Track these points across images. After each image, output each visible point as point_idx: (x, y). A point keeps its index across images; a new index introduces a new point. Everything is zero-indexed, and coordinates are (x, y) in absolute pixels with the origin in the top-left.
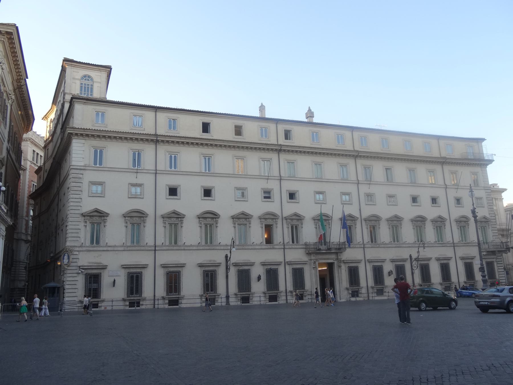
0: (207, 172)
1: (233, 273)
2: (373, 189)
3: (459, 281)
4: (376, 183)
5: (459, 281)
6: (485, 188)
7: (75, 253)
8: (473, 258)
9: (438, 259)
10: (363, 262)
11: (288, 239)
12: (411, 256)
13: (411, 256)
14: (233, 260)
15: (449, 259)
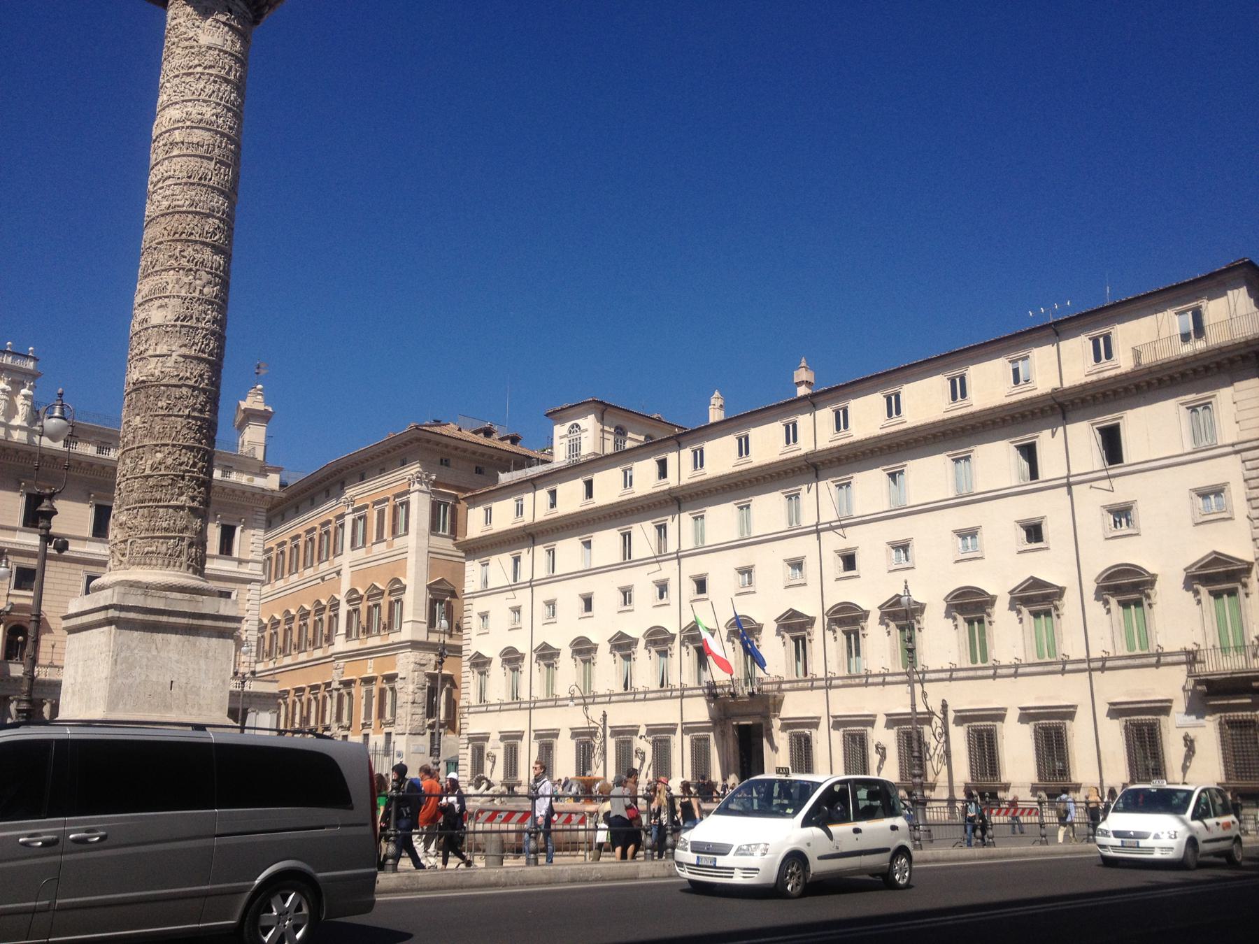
0: (627, 560)
1: (611, 744)
2: (855, 538)
3: (1102, 781)
4: (860, 519)
5: (1102, 781)
6: (1238, 448)
7: (466, 715)
8: (1163, 708)
9: (1027, 716)
10: (824, 725)
11: (689, 679)
12: (945, 706)
13: (945, 706)
14: (611, 722)
15: (1068, 713)
